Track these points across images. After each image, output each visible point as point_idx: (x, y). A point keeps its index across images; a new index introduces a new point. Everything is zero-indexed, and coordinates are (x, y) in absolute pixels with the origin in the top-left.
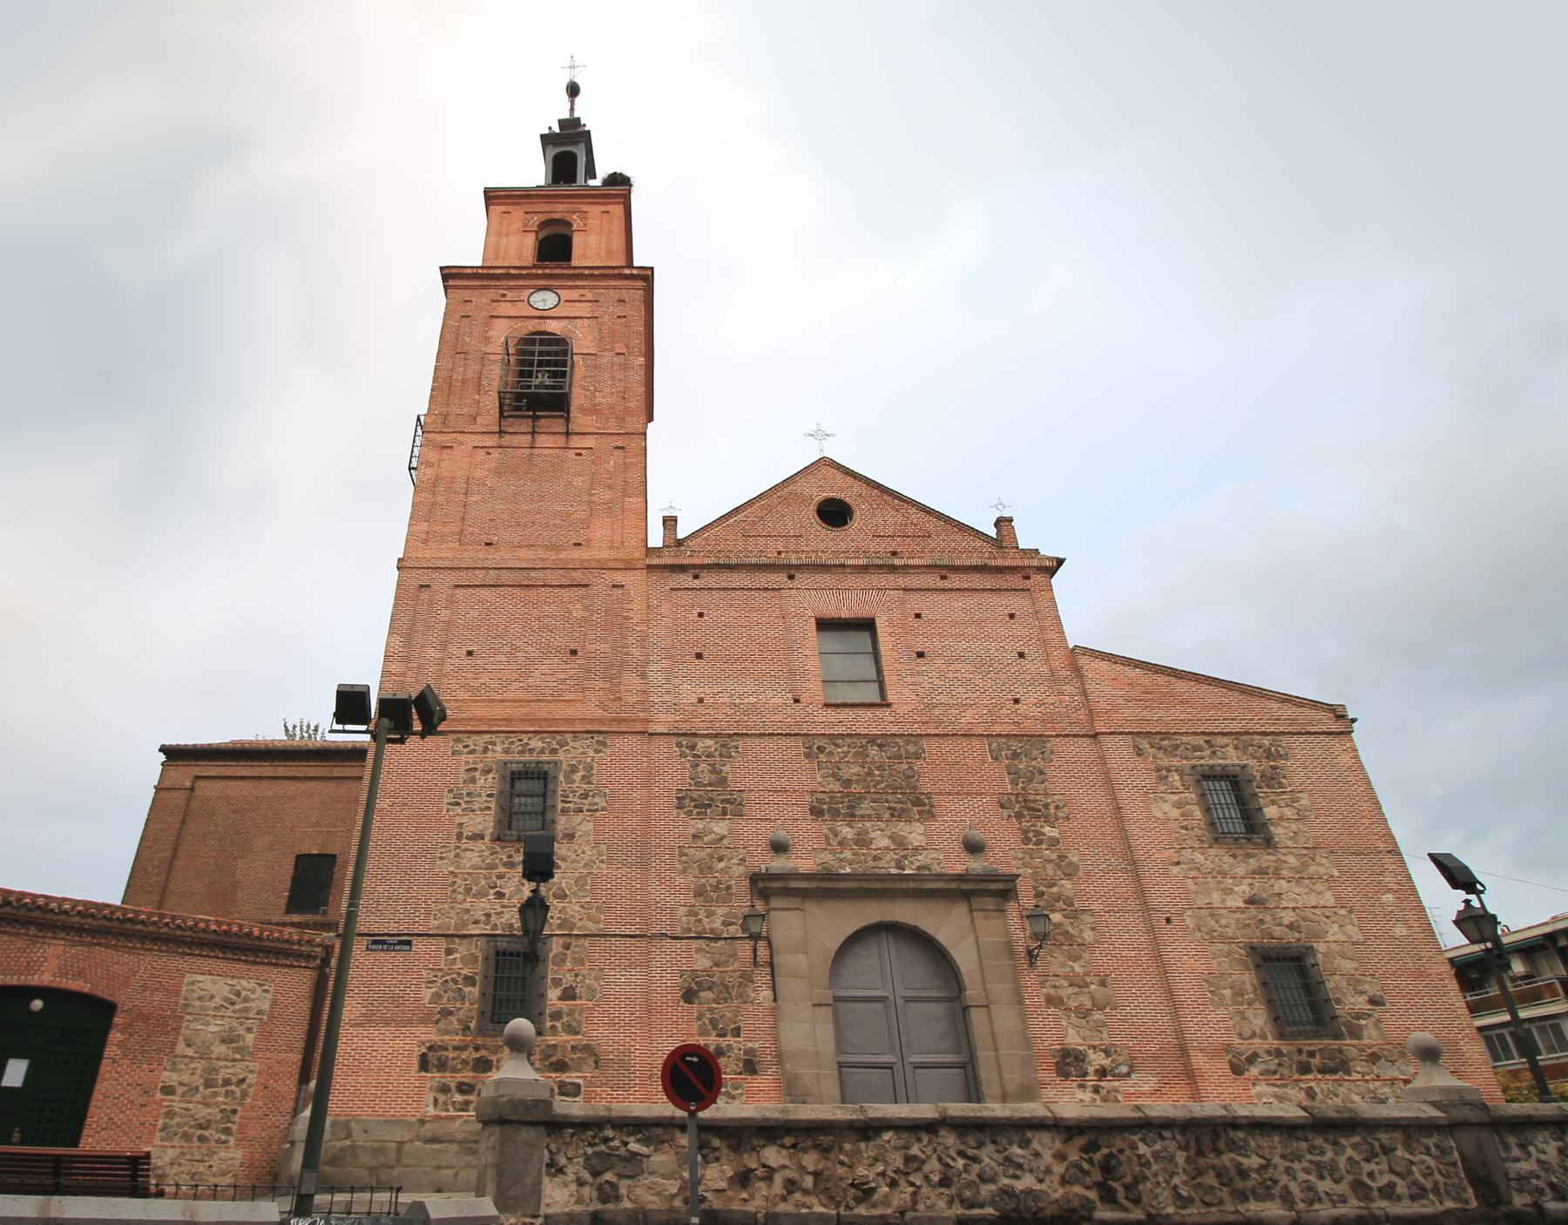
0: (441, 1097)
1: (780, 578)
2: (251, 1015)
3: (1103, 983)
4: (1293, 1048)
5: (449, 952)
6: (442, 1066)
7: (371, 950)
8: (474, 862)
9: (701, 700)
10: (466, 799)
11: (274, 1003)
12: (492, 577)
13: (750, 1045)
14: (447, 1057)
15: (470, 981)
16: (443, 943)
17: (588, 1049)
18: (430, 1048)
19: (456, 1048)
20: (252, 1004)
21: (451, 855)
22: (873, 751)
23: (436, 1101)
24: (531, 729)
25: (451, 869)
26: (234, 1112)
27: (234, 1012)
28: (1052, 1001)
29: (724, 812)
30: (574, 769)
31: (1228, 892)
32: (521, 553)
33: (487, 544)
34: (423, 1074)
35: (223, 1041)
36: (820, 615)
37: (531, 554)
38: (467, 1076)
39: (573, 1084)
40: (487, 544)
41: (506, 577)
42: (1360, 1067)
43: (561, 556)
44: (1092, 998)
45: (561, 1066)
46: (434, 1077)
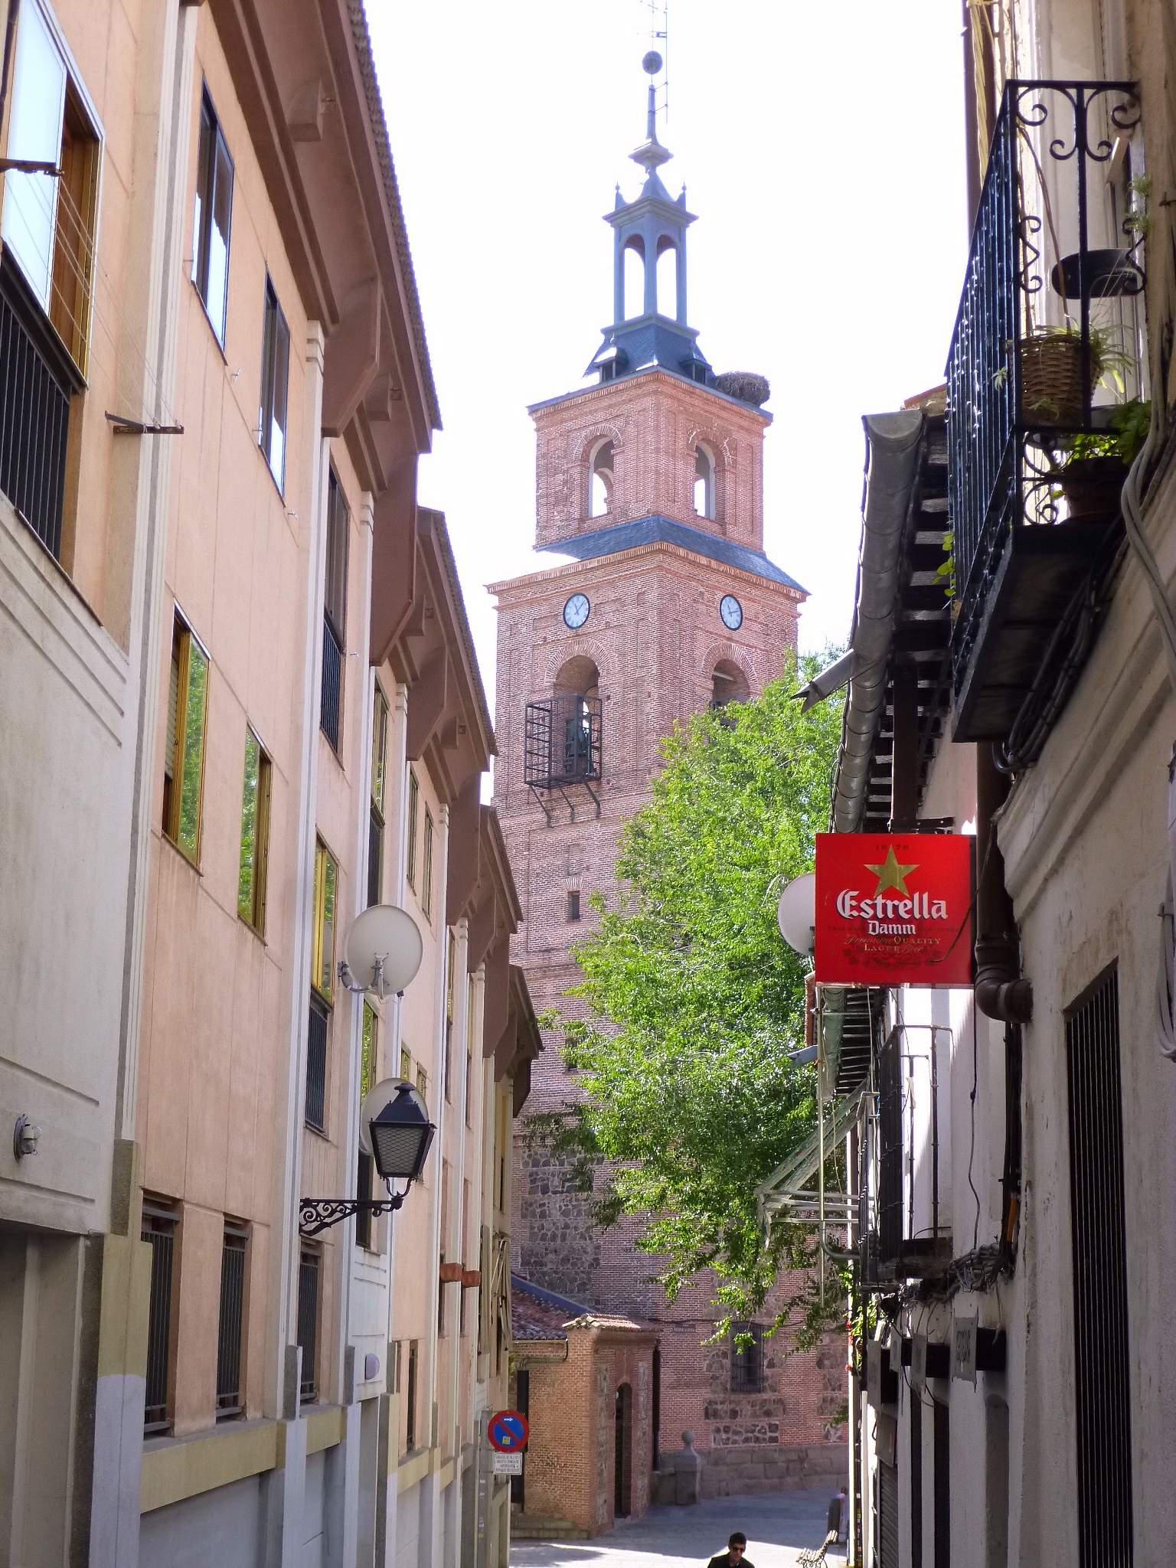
15: (725, 1355)
17: (780, 1401)
18: (710, 1403)
19: (722, 1403)
38: (727, 1421)
45: (768, 1414)
46: (713, 1424)
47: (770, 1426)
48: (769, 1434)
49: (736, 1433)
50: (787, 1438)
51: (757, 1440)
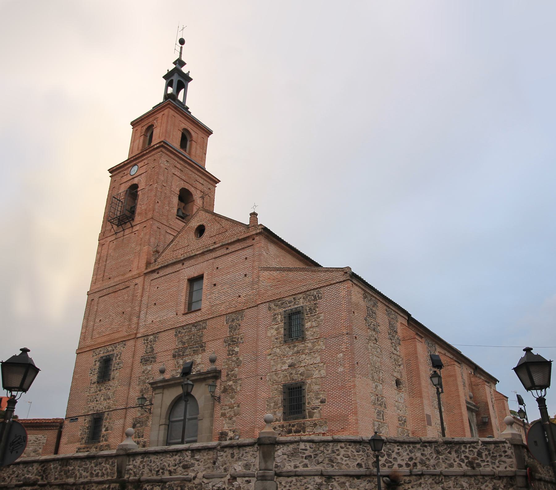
1: (179, 266)
2: (41, 444)
3: (238, 406)
4: (288, 424)
5: (85, 420)
9: (152, 321)
11: (47, 440)
13: (145, 440)
20: (41, 441)
21: (88, 390)
22: (193, 329)
24: (109, 344)
27: (36, 444)
28: (223, 415)
30: (117, 355)
31: (284, 363)
33: (110, 278)
35: (34, 452)
36: (189, 278)
43: (125, 277)
44: (234, 412)
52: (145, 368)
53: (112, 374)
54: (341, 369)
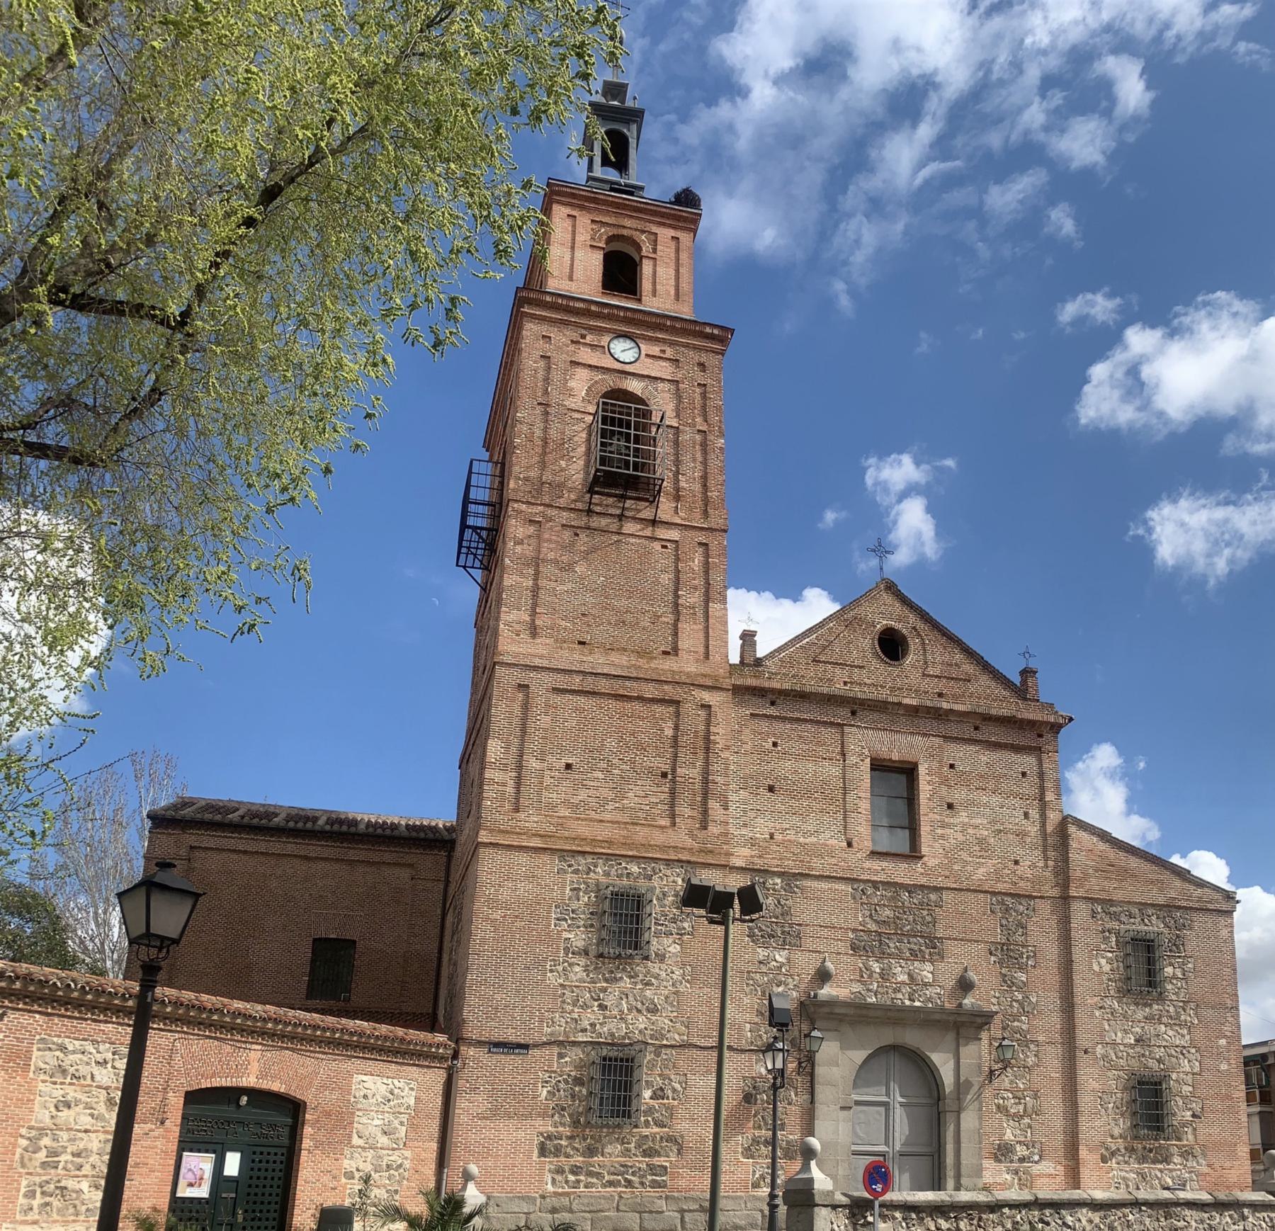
0: (559, 1178)
3: (1036, 1097)
5: (561, 1056)
6: (558, 1151)
7: (493, 1053)
8: (579, 976)
9: (772, 836)
10: (571, 915)
12: (589, 684)
14: (561, 1146)
16: (556, 1050)
17: (671, 1139)
18: (549, 1138)
20: (403, 1101)
23: (554, 1180)
24: (630, 853)
25: (561, 981)
26: (396, 1192)
29: (784, 943)
32: (615, 658)
33: (580, 643)
34: (543, 1159)
37: (623, 660)
39: (662, 1166)
40: (580, 643)
41: (603, 685)
42: (1177, 1159)
46: (550, 1162)
47: (652, 1169)
48: (650, 1178)
49: (590, 1174)
50: (682, 1183)
51: (629, 1183)
52: (762, 953)
53: (654, 942)
54: (1224, 1067)
